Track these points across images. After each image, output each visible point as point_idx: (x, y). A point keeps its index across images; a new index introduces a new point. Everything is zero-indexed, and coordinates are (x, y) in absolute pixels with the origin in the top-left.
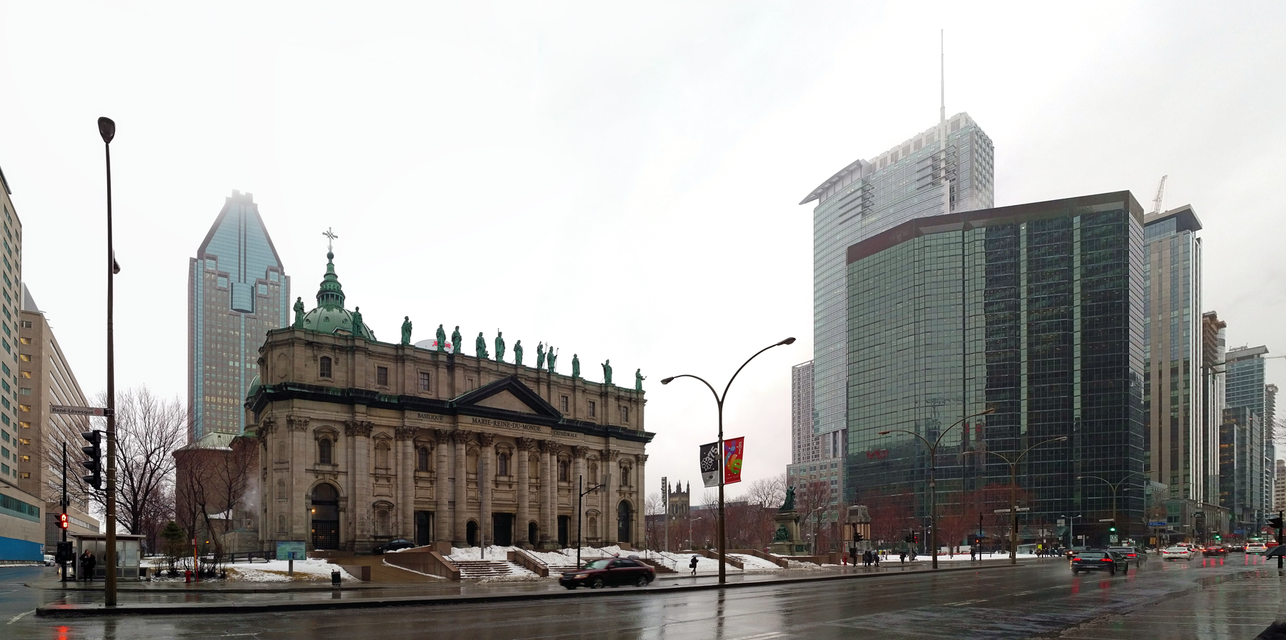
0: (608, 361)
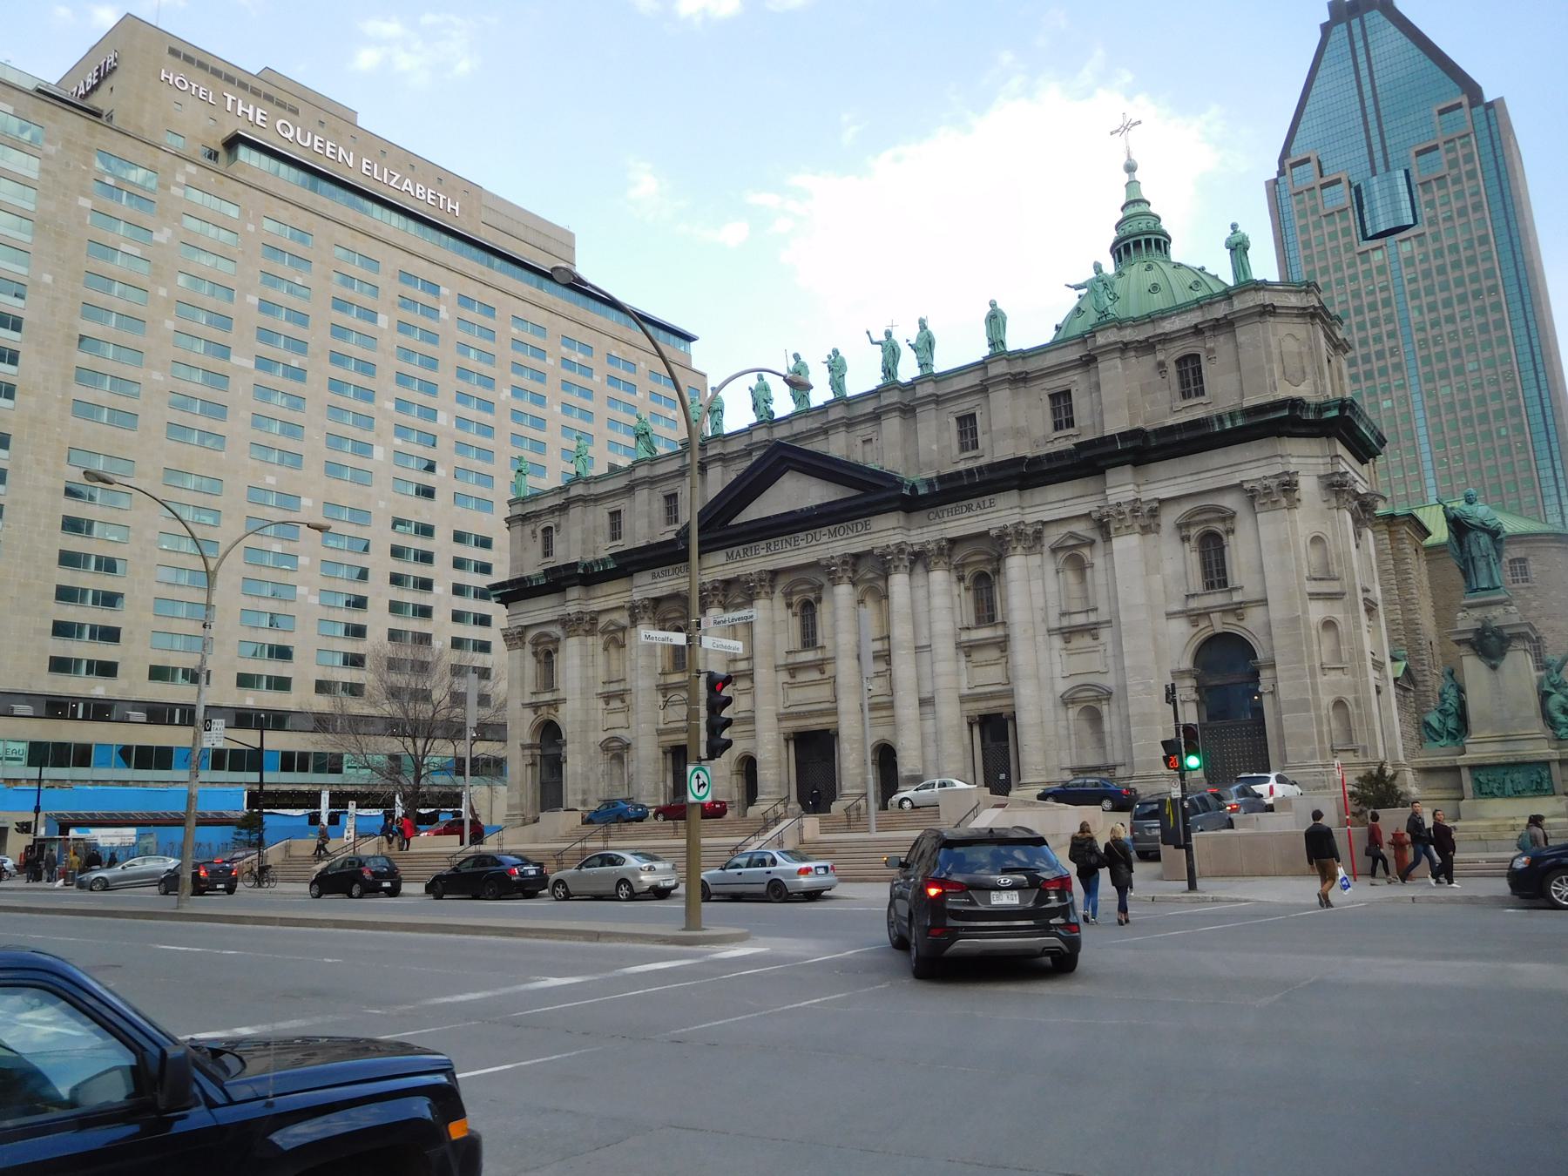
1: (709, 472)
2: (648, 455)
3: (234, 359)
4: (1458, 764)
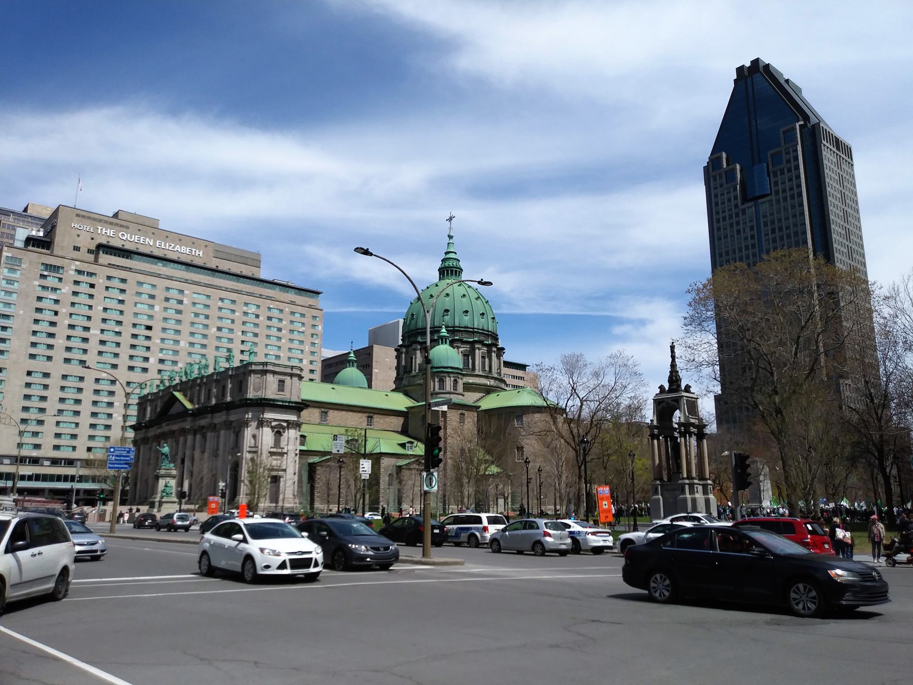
3: (92, 331)
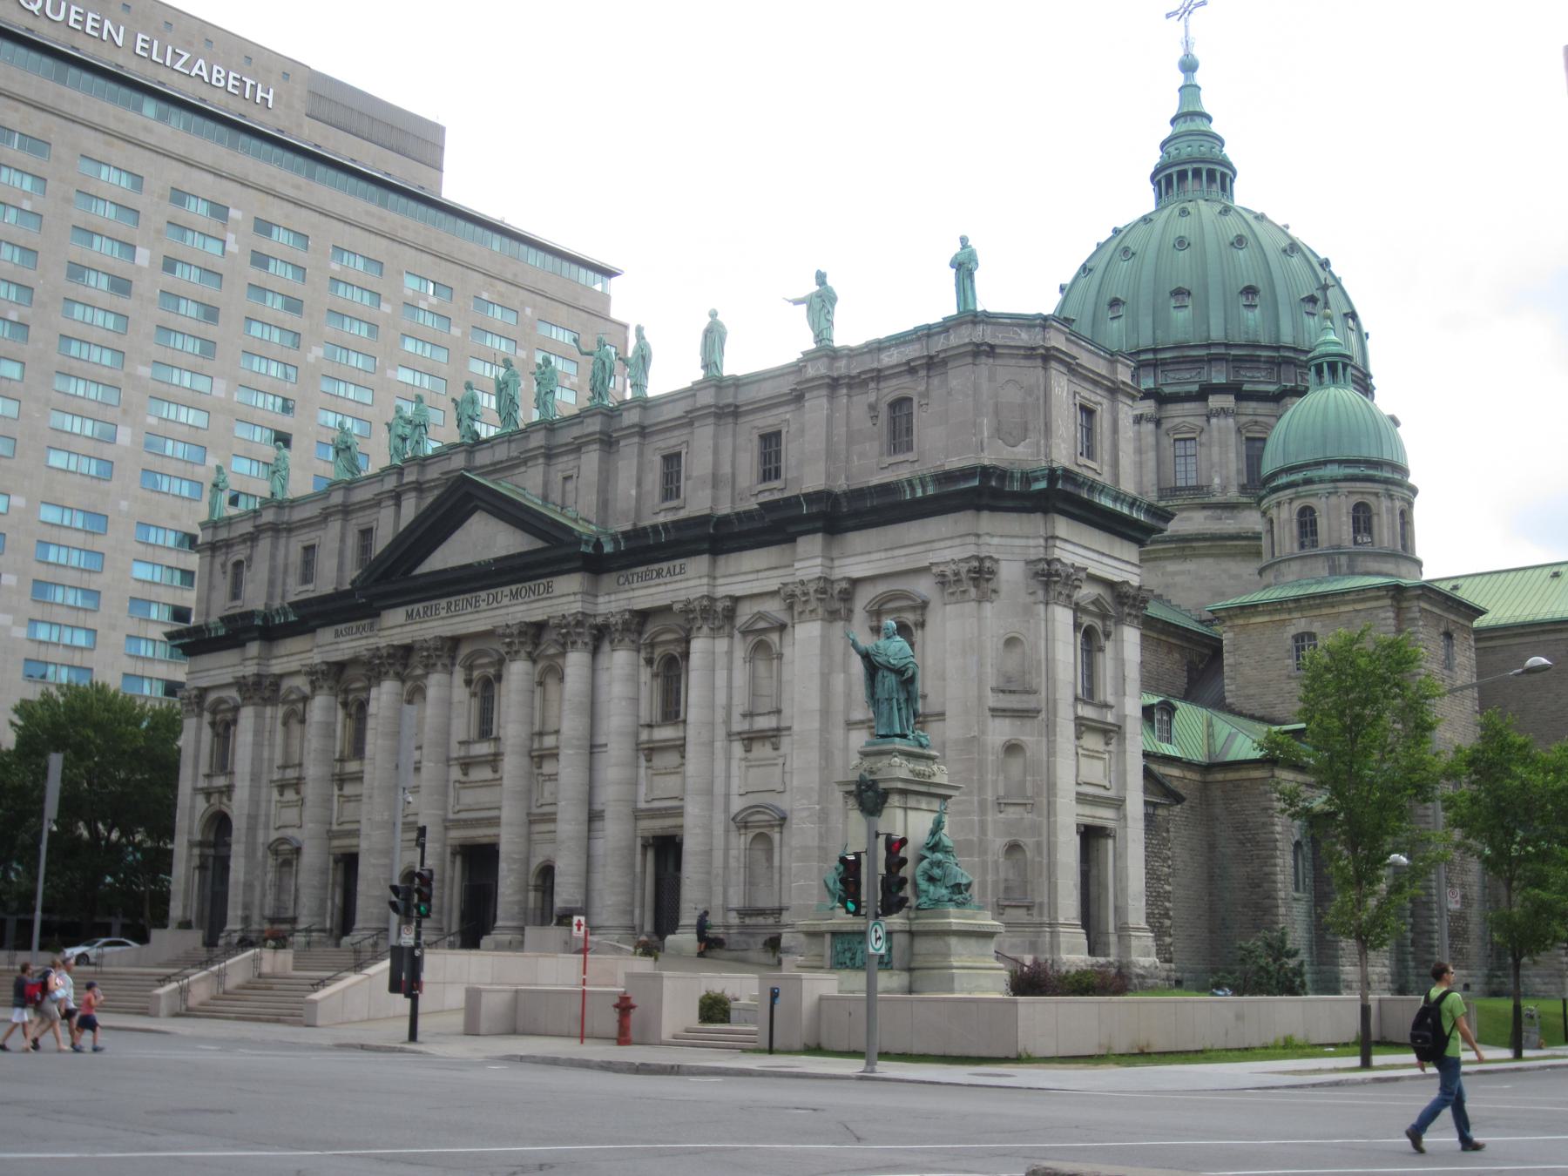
0: (821, 278)
1: (404, 504)
2: (348, 477)
4: (824, 928)
